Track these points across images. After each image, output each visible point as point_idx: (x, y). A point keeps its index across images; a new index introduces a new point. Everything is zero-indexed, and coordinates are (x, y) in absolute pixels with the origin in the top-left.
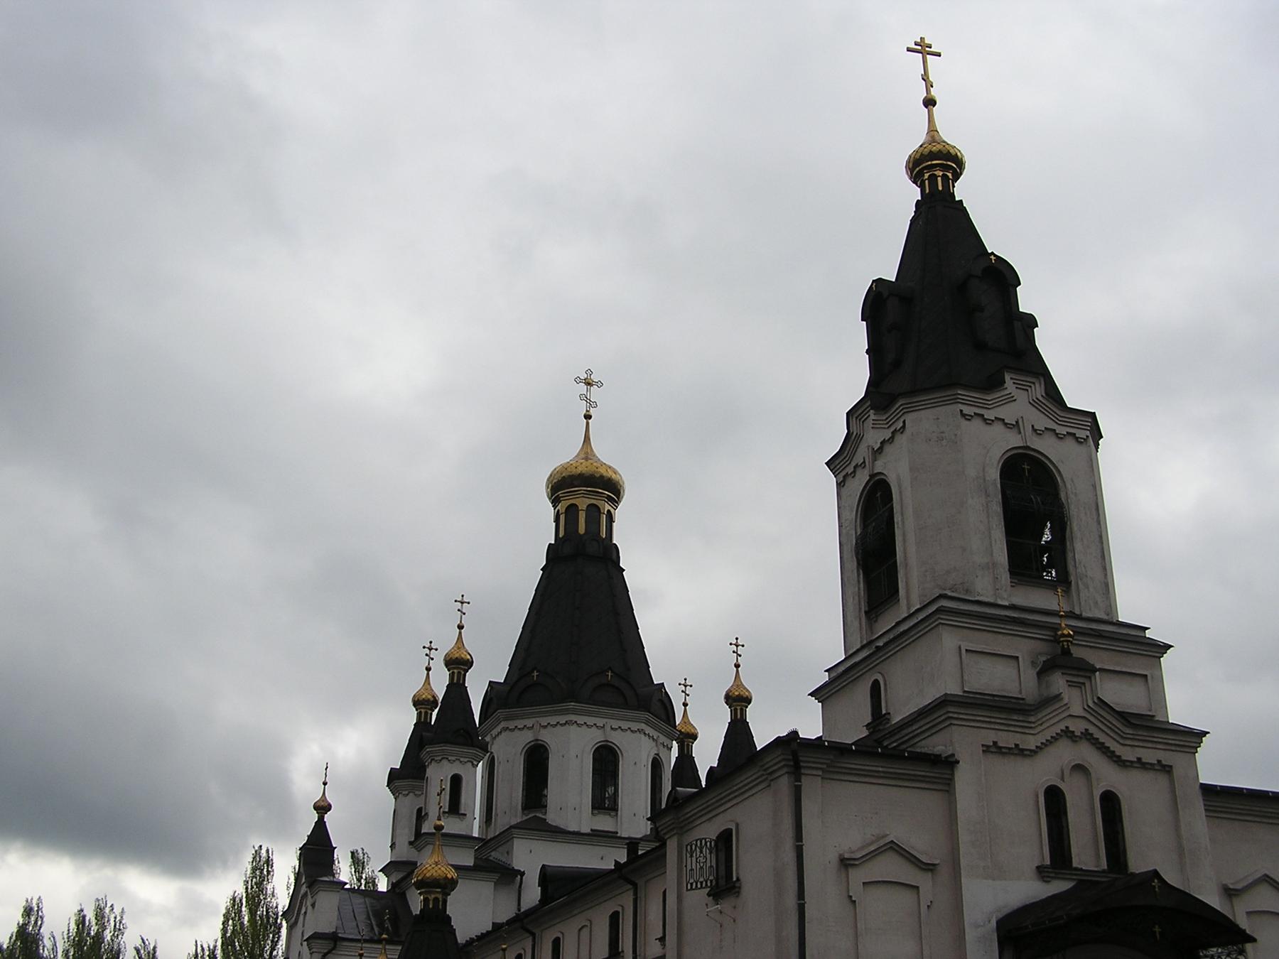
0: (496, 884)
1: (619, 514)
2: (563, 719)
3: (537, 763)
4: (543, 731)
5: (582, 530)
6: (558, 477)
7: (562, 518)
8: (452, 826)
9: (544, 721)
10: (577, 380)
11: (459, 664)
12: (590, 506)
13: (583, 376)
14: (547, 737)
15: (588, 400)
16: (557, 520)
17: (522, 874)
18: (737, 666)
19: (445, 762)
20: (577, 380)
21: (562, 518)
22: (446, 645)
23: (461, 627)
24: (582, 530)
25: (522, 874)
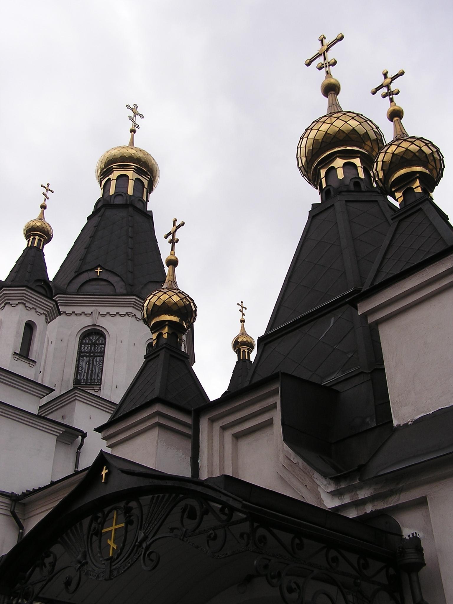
0: (58, 437)
1: (151, 196)
2: (123, 311)
3: (93, 342)
4: (101, 319)
5: (130, 192)
6: (114, 152)
7: (113, 184)
8: (22, 369)
9: (104, 310)
10: (128, 107)
11: (39, 234)
12: (136, 179)
13: (132, 107)
14: (104, 323)
15: (134, 122)
16: (106, 188)
17: (84, 435)
18: (243, 321)
19: (21, 306)
20: (128, 107)
21: (113, 184)
22: (31, 216)
23: (43, 207)
24: (130, 192)
25: (84, 435)
